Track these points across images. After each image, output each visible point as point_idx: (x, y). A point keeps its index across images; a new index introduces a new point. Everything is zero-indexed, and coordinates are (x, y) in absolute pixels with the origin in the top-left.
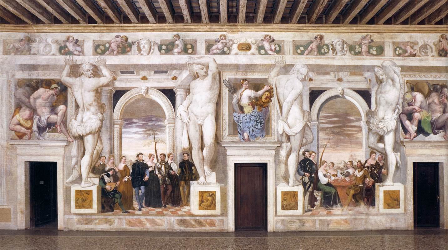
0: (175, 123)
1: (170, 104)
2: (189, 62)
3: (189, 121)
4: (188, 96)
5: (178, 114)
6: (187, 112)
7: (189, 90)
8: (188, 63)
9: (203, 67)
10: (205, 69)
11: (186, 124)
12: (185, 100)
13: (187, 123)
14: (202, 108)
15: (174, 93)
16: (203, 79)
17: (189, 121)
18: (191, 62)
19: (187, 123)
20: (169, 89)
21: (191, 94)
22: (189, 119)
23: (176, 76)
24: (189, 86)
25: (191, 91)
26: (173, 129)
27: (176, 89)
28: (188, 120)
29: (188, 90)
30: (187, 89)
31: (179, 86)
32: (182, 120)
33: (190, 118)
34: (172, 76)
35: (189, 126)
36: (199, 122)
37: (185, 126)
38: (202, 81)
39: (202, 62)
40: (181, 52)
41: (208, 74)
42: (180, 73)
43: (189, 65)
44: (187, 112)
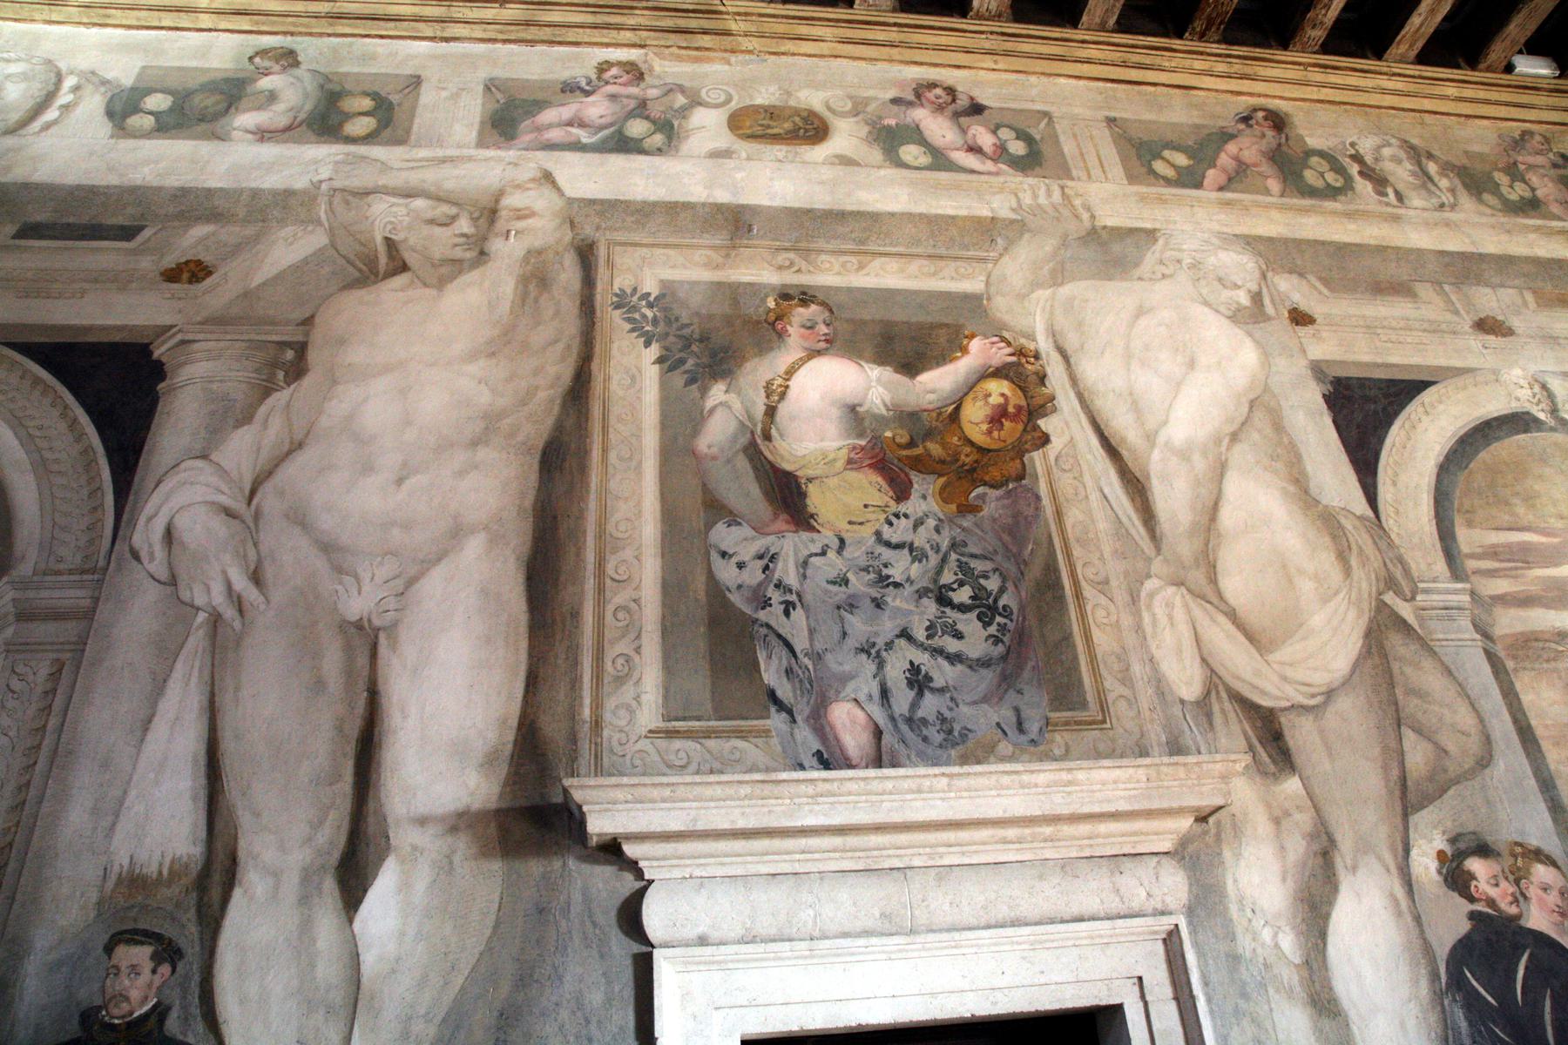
0: (88, 615)
1: (87, 450)
2: (337, 184)
3: (251, 594)
4: (280, 398)
5: (147, 534)
6: (248, 515)
7: (301, 349)
8: (324, 186)
9: (454, 211)
10: (464, 225)
11: (216, 619)
12: (246, 418)
13: (229, 613)
14: (400, 482)
15: (158, 371)
16: (442, 283)
17: (251, 594)
18: (355, 183)
19: (229, 613)
20: (117, 338)
21: (307, 381)
22: (256, 578)
23: (207, 258)
24: (308, 322)
25: (313, 355)
26: (55, 676)
27: (183, 342)
28: (241, 583)
29: (290, 354)
30: (283, 345)
31: (219, 321)
32: (173, 581)
33: (269, 573)
34: (169, 261)
35: (238, 643)
36: (356, 606)
37: (197, 640)
38: (433, 292)
39: (449, 185)
40: (288, 129)
41: (482, 253)
42: (256, 239)
43: (337, 200)
44: (248, 515)
